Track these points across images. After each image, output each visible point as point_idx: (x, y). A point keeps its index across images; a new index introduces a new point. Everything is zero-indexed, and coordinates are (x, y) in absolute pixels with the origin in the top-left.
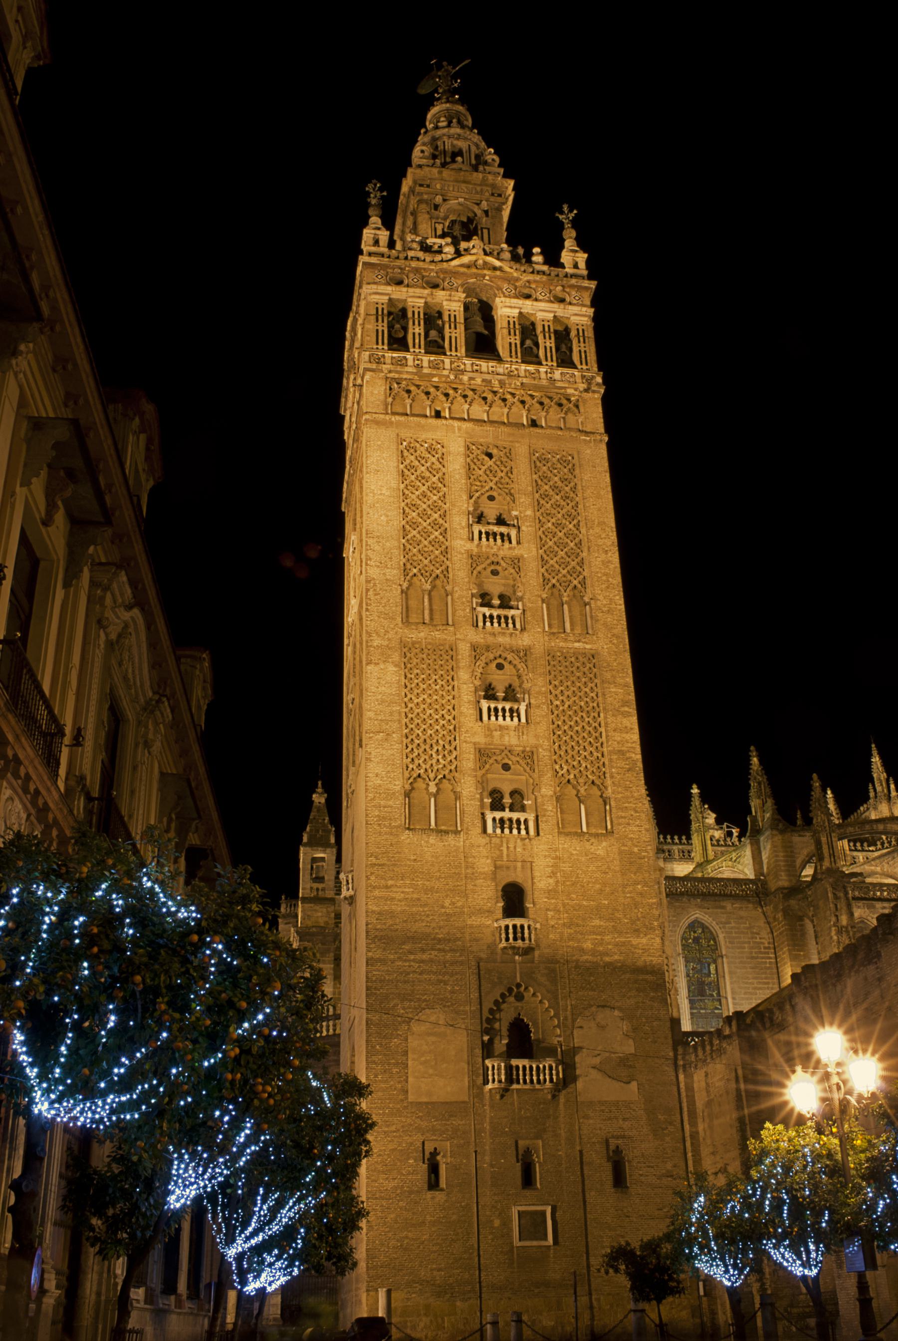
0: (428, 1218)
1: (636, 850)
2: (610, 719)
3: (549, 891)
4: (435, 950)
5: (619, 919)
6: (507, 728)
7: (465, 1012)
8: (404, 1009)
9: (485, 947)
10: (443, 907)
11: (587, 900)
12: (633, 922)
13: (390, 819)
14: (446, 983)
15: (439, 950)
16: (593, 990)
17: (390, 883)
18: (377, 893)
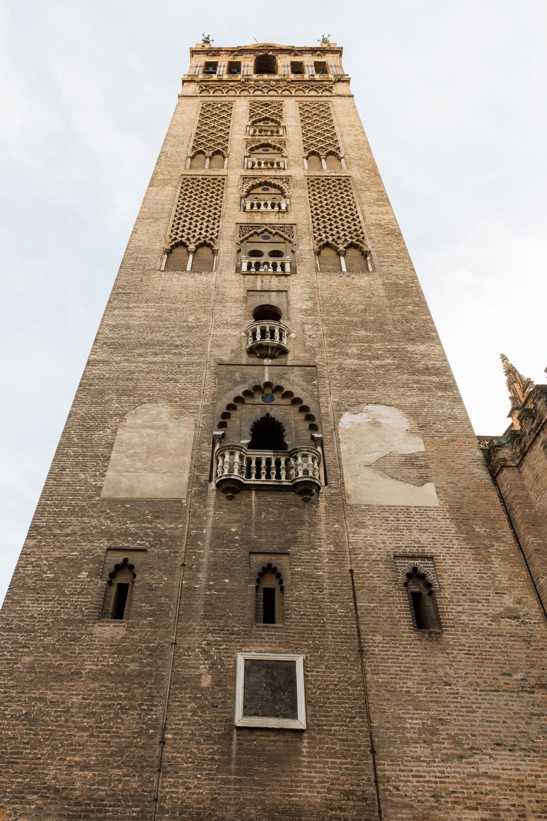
0: (89, 666)
1: (402, 282)
2: (365, 208)
3: (306, 310)
4: (171, 354)
5: (390, 331)
6: (269, 212)
7: (197, 407)
8: (120, 403)
9: (229, 352)
10: (185, 321)
11: (350, 316)
12: (405, 333)
13: (145, 265)
14: (176, 381)
15: (175, 353)
16: (361, 388)
17: (132, 305)
18: (116, 312)
